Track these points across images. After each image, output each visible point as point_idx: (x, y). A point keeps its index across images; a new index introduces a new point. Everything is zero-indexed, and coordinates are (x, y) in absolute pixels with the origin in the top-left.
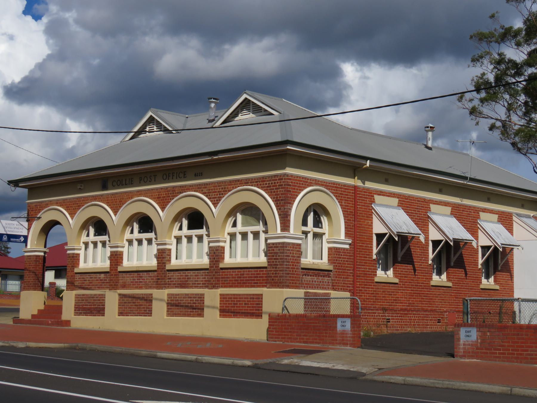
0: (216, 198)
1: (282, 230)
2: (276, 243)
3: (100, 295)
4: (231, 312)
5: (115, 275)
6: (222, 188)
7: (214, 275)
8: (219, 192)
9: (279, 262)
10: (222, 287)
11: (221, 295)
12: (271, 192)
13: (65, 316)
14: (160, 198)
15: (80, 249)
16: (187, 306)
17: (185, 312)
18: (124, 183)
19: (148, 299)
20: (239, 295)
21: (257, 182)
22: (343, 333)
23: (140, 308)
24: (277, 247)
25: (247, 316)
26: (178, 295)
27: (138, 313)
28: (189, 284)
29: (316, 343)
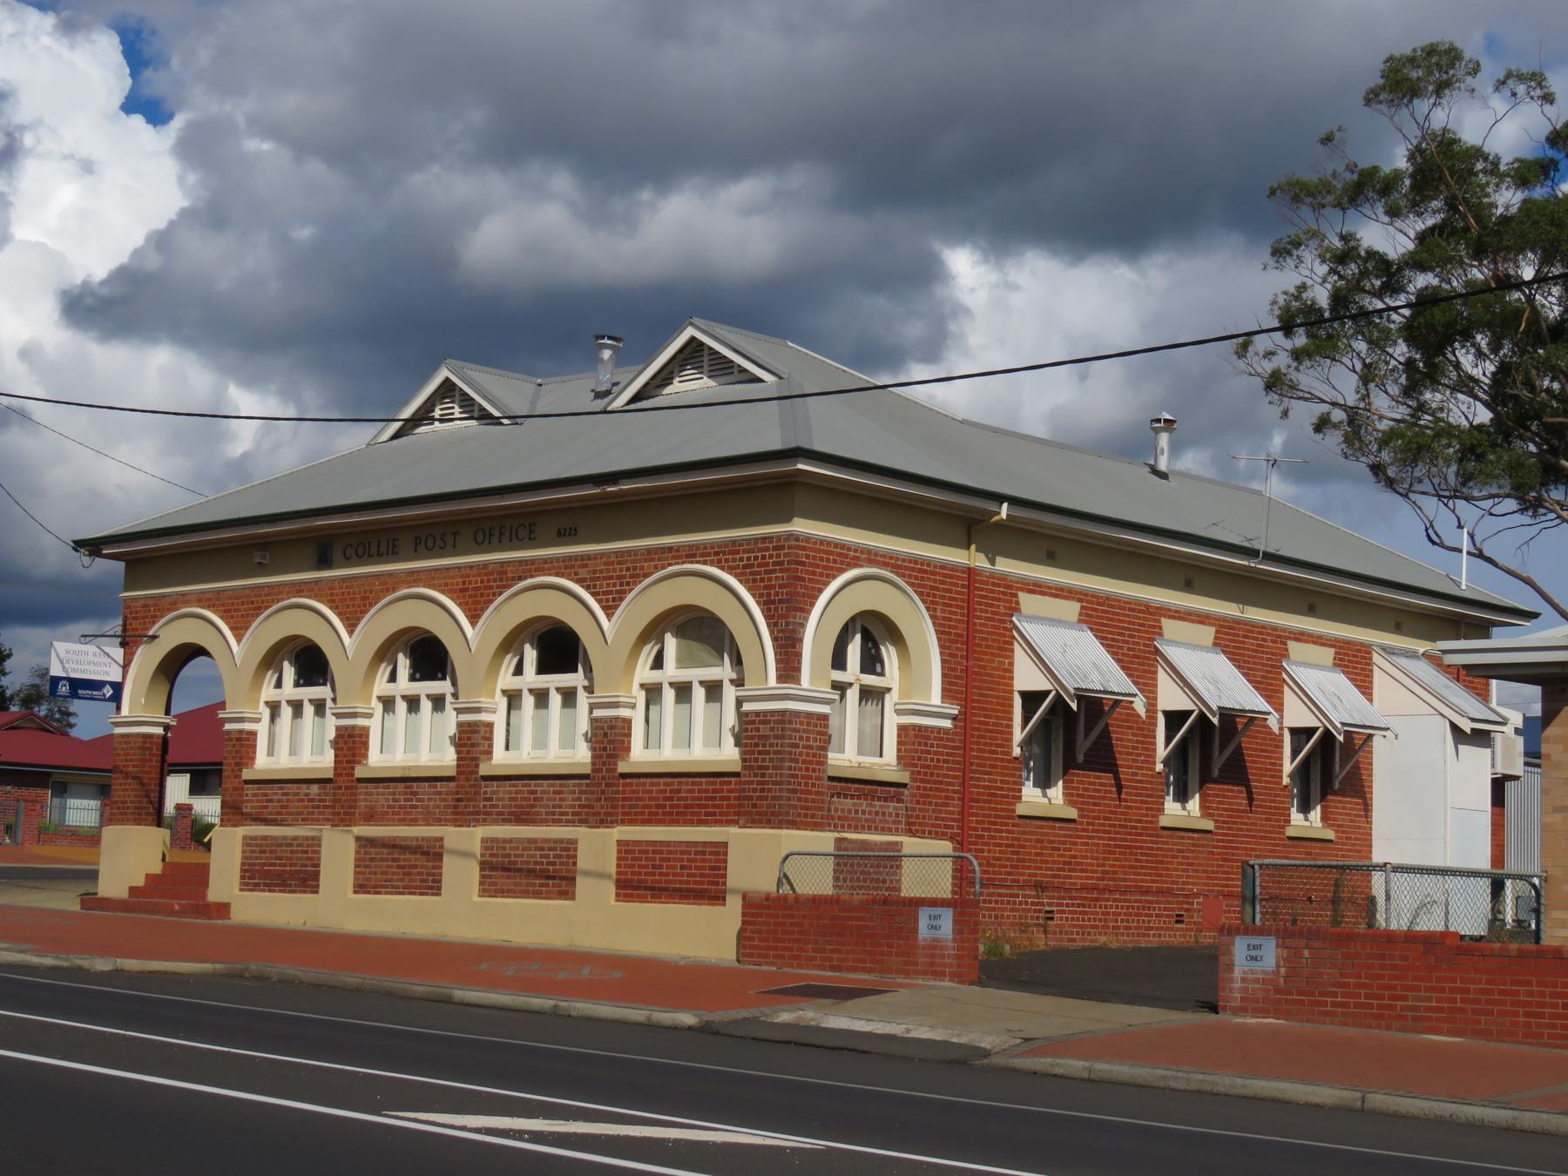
0: (610, 592)
1: (781, 678)
2: (765, 713)
3: (307, 838)
4: (646, 888)
7: (603, 792)
8: (618, 577)
9: (771, 760)
10: (623, 822)
11: (619, 843)
12: (755, 581)
13: (215, 894)
14: (467, 590)
15: (258, 720)
16: (534, 871)
17: (528, 885)
18: (374, 550)
19: (432, 853)
20: (668, 844)
21: (717, 554)
22: (934, 945)
24: (766, 722)
25: (687, 898)
26: (511, 841)
28: (538, 813)
29: (864, 970)
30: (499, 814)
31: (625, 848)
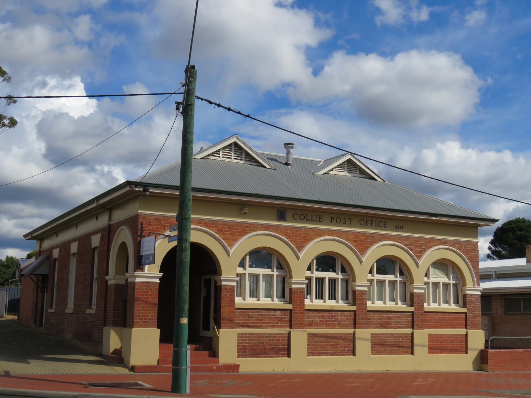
0: (417, 251)
3: (278, 334)
5: (300, 313)
6: (423, 244)
7: (419, 318)
8: (420, 246)
11: (429, 335)
14: (357, 241)
17: (391, 350)
18: (309, 218)
21: (454, 244)
23: (337, 347)
24: (474, 298)
25: (453, 352)
26: (383, 334)
28: (391, 324)
30: (374, 324)
31: (430, 336)
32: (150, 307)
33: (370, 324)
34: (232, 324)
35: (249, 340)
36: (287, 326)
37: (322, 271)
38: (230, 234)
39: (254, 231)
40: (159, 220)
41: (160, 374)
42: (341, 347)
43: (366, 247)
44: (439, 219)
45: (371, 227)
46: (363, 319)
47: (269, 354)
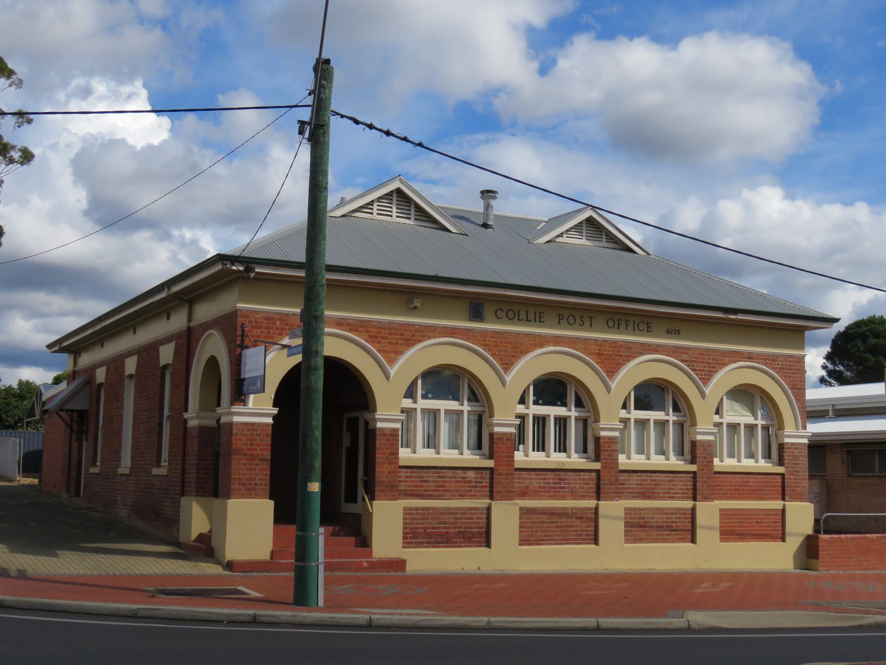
0: (703, 371)
3: (471, 509)
5: (506, 474)
6: (713, 359)
7: (705, 482)
8: (708, 363)
11: (721, 510)
14: (602, 354)
16: (662, 526)
17: (658, 535)
18: (523, 315)
21: (765, 359)
25: (761, 538)
26: (645, 509)
27: (562, 540)
28: (658, 493)
30: (631, 493)
31: (724, 513)
32: (257, 465)
33: (624, 493)
34: (395, 493)
35: (422, 519)
36: (486, 496)
37: (544, 404)
38: (390, 343)
39: (430, 338)
40: (272, 319)
41: (275, 574)
42: (574, 531)
43: (616, 364)
44: (740, 317)
45: (626, 331)
46: (611, 484)
47: (456, 542)
